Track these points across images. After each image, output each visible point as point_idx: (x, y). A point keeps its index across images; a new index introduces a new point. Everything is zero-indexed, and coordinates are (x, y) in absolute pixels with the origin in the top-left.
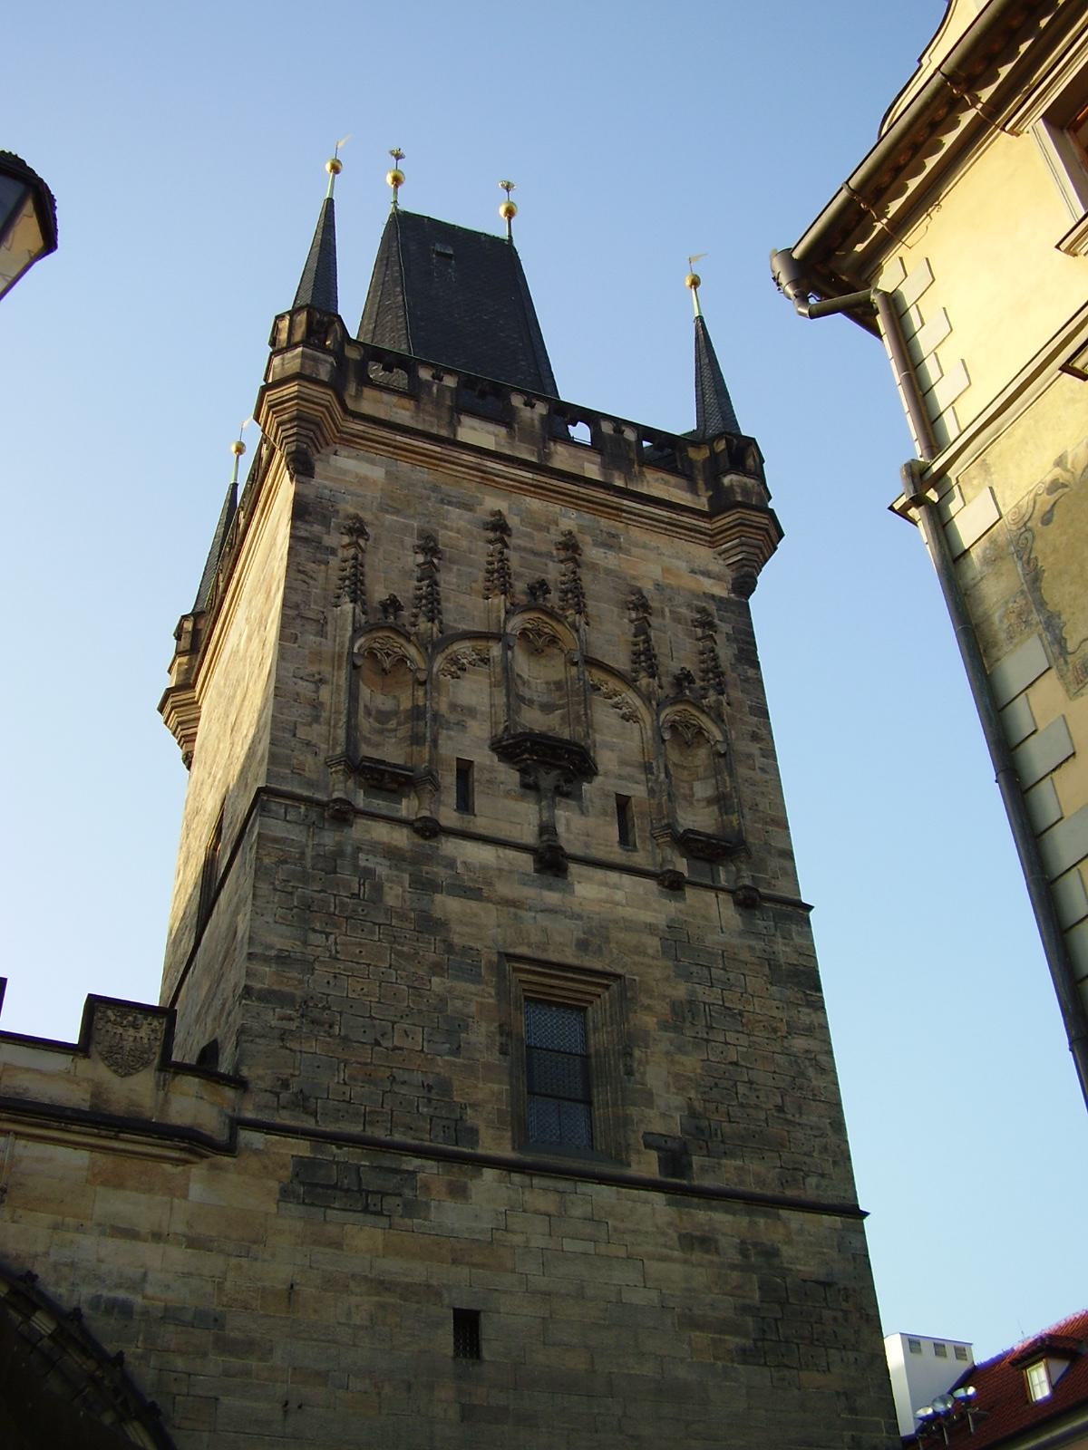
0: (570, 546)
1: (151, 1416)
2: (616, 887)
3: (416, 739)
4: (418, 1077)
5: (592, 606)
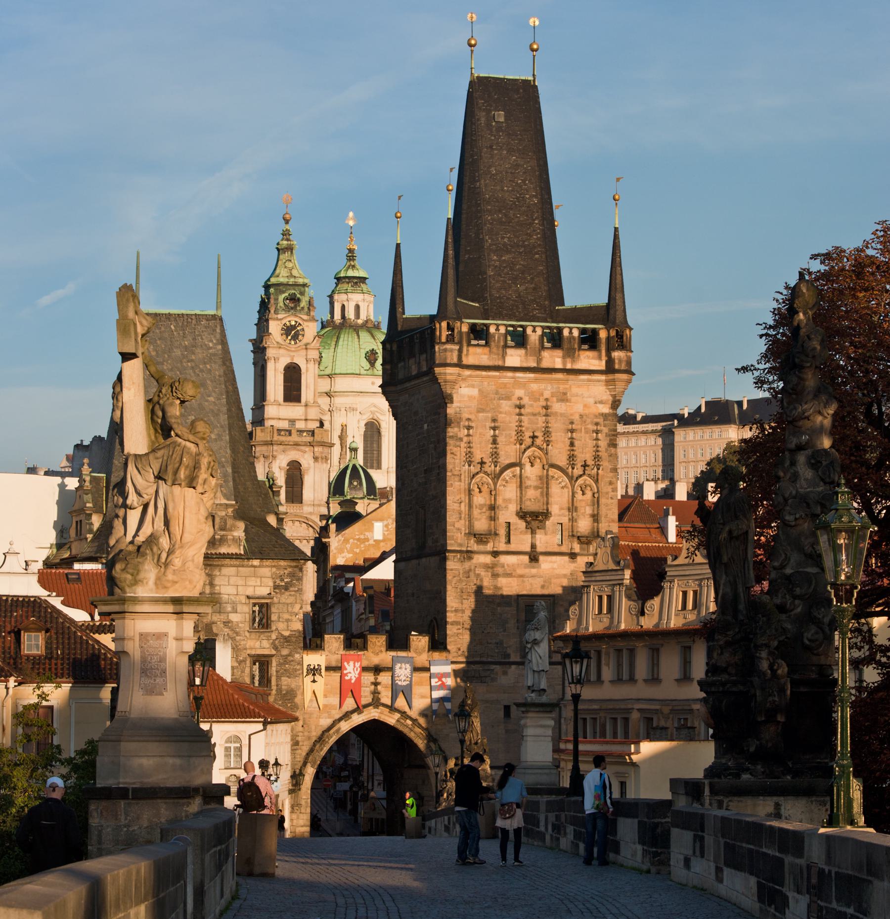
0: (546, 408)
2: (555, 562)
4: (494, 641)
5: (554, 437)
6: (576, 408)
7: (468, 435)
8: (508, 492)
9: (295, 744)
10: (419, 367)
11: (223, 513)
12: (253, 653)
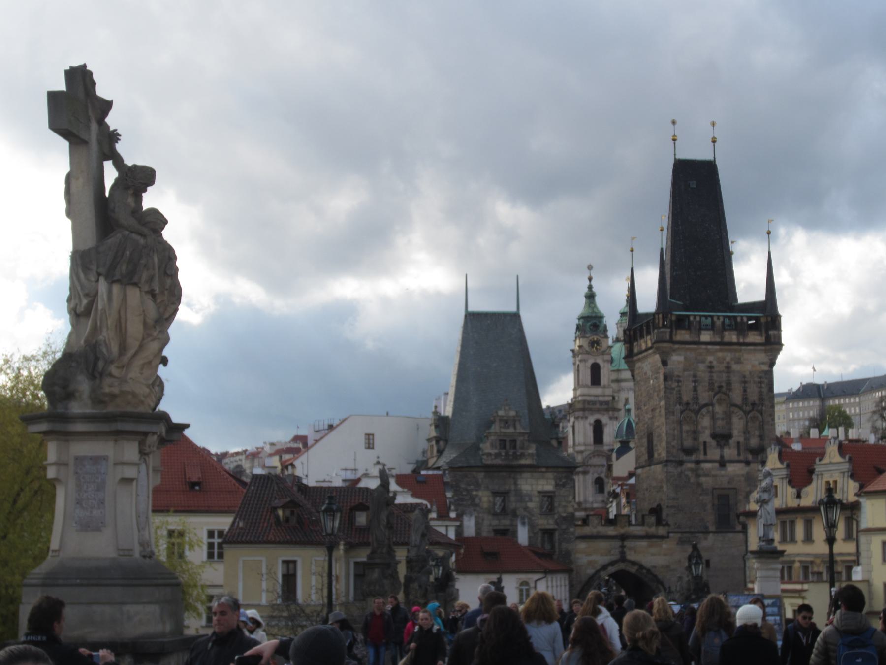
0: (728, 367)
1: (662, 583)
3: (695, 439)
6: (747, 368)
7: (678, 386)
8: (706, 422)
9: (571, 586)
10: (647, 344)
11: (521, 438)
12: (543, 527)
